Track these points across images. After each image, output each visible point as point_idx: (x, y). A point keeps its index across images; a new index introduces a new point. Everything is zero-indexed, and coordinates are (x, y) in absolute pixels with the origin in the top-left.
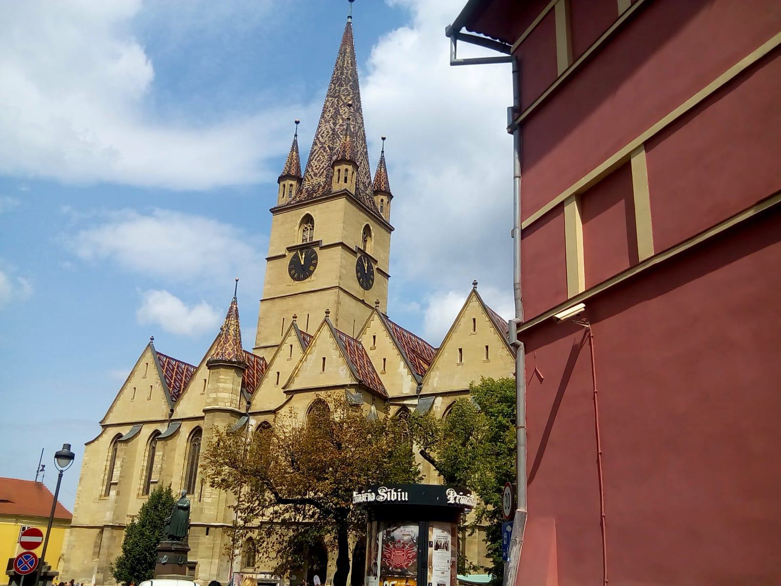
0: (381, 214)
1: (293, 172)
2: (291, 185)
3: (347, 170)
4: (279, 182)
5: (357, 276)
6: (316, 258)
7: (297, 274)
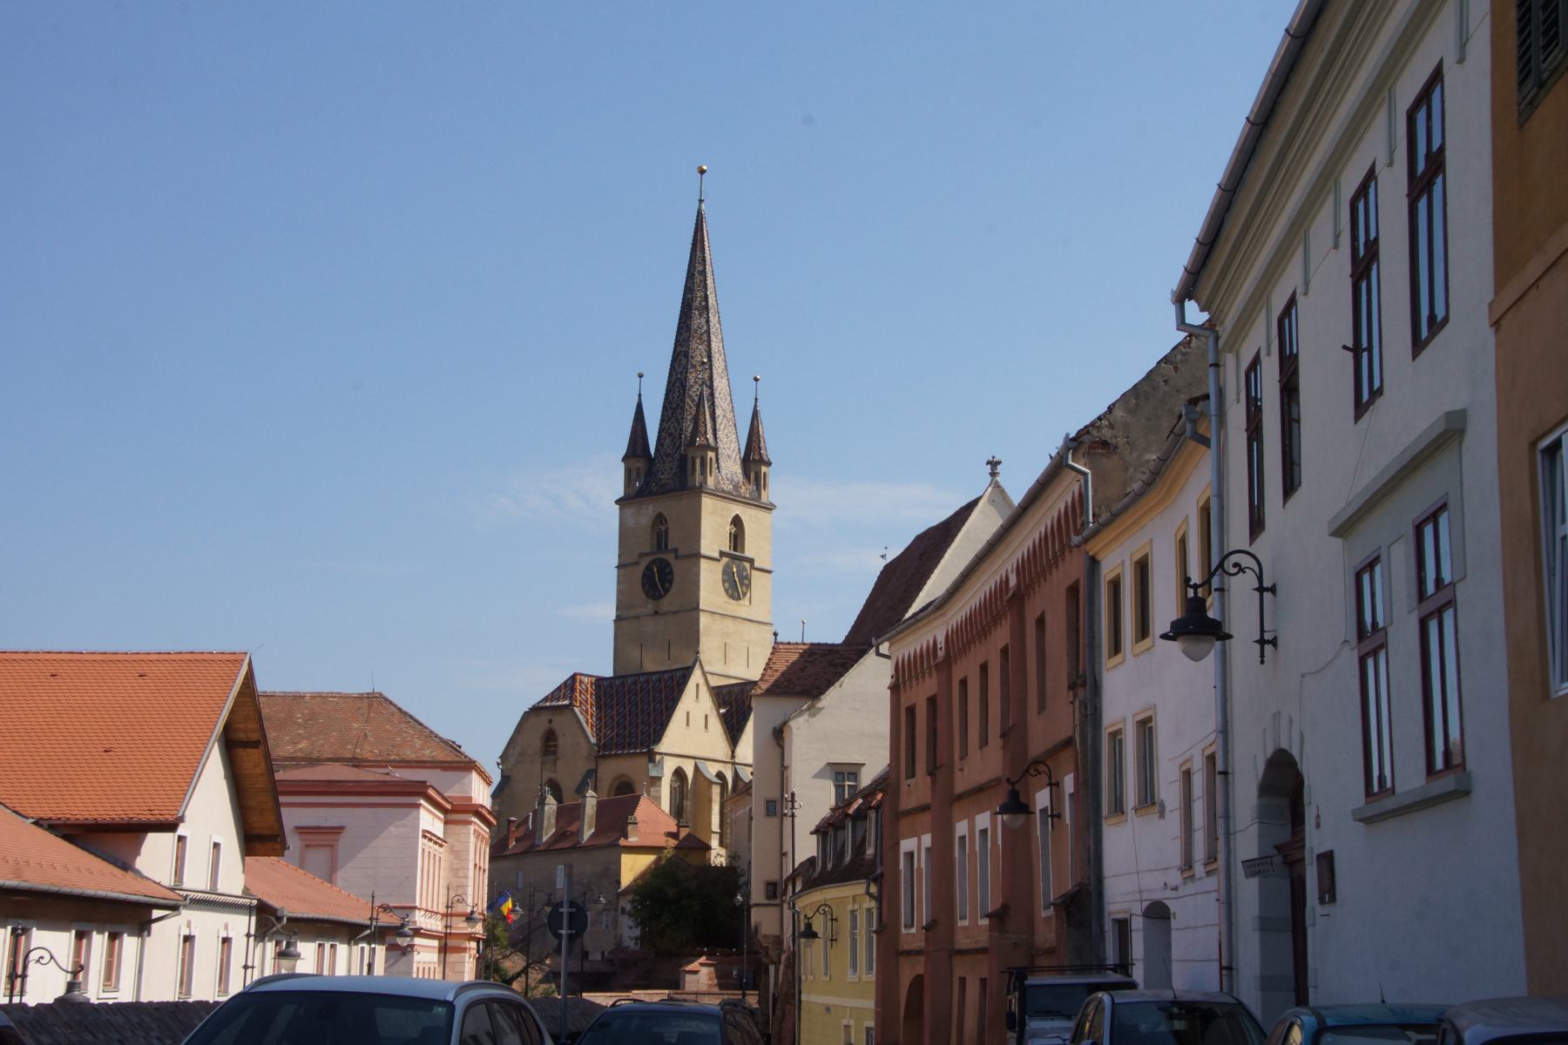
5: (725, 589)
6: (671, 572)
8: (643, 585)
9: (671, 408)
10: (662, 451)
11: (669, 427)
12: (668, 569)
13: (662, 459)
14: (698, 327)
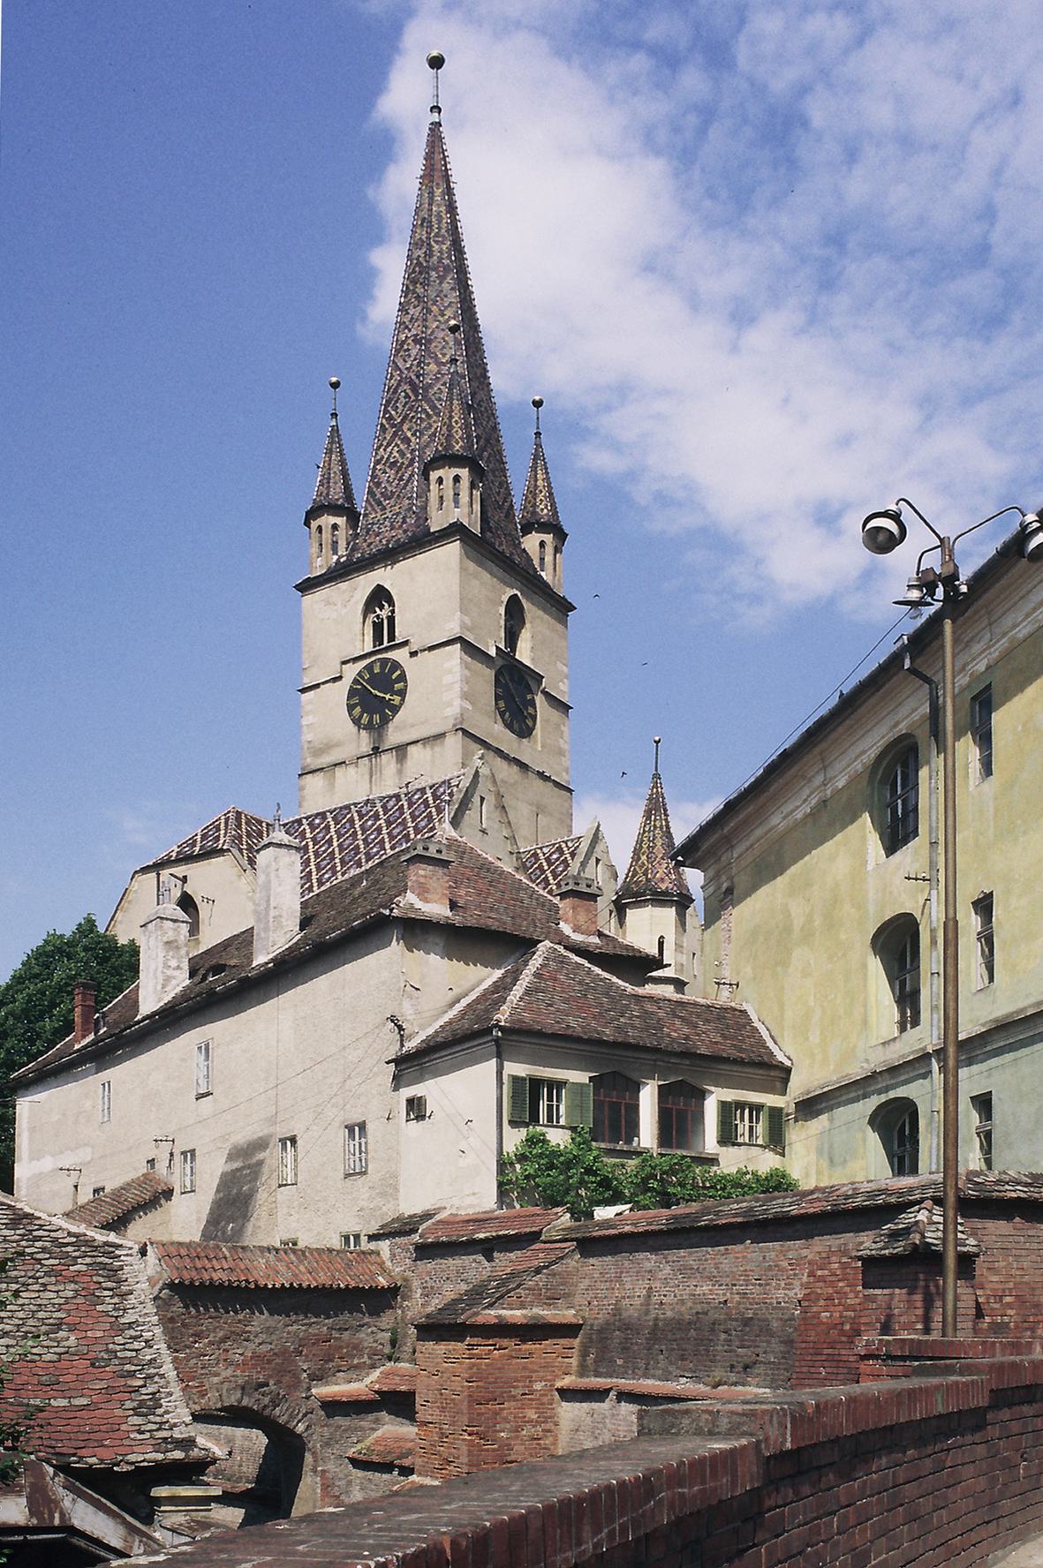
0: (543, 574)
1: (337, 493)
2: (335, 527)
3: (457, 479)
4: (307, 524)
6: (403, 678)
7: (365, 715)
8: (350, 708)
9: (393, 426)
10: (377, 492)
11: (391, 453)
12: (398, 672)
13: (379, 503)
14: (437, 296)
